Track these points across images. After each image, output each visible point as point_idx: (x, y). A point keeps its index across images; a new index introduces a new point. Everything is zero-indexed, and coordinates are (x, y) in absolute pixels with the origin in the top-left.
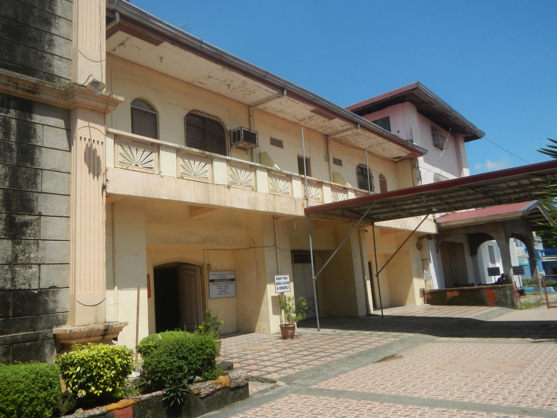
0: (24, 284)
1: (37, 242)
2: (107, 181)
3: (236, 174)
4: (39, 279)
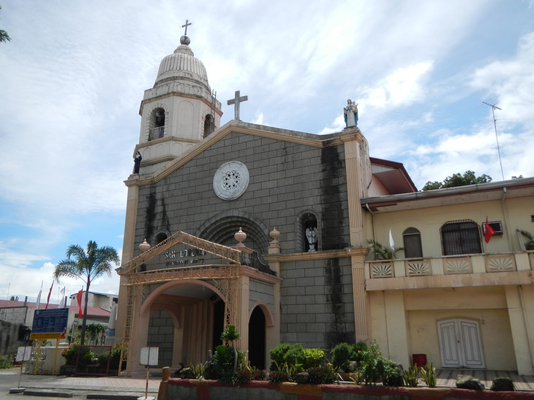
0: (340, 330)
1: (344, 314)
2: (366, 285)
3: (452, 264)
4: (346, 328)
